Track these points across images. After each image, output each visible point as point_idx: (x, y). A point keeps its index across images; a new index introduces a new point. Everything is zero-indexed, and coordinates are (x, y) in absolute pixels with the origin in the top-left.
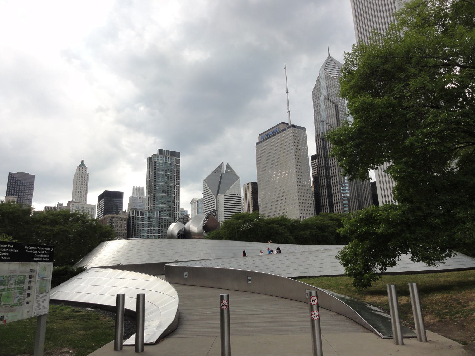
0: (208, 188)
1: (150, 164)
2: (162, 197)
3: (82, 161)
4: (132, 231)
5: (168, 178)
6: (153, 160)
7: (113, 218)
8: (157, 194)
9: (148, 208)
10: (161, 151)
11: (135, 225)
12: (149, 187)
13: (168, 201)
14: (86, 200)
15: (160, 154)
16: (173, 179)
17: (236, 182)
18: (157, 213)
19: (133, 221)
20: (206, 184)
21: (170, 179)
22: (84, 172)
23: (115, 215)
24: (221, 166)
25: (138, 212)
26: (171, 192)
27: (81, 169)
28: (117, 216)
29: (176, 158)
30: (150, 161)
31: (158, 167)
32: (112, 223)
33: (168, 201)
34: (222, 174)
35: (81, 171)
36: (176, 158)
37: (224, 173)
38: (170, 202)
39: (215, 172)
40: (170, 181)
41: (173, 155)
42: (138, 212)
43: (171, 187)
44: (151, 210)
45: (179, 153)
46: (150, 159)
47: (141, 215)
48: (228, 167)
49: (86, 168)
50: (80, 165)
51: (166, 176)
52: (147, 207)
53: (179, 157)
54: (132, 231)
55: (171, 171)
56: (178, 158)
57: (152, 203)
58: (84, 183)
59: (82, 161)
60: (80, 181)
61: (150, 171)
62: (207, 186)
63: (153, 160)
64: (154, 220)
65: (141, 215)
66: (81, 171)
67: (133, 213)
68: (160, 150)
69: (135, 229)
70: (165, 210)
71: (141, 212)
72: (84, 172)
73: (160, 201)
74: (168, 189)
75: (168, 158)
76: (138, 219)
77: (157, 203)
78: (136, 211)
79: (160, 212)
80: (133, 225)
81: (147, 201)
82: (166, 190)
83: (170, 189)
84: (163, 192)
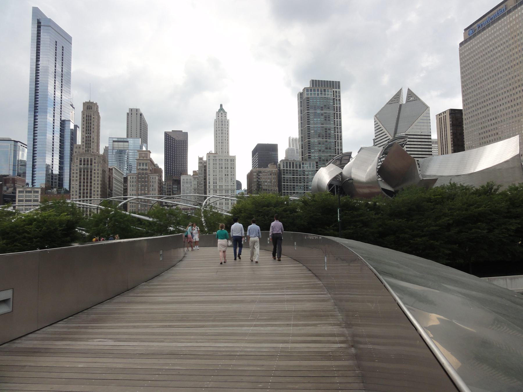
0: (381, 126)
1: (301, 102)
2: (319, 144)
3: (221, 106)
4: (284, 187)
5: (325, 117)
6: (305, 96)
7: (260, 172)
8: (312, 140)
9: (302, 158)
10: (314, 83)
11: (287, 180)
12: (302, 132)
13: (326, 148)
14: (228, 152)
15: (313, 85)
16: (332, 118)
17: (424, 114)
18: (313, 164)
19: (284, 175)
20: (378, 121)
21: (327, 119)
22: (223, 118)
23: (262, 169)
24: (398, 96)
25: (290, 163)
26: (329, 137)
27: (220, 115)
28: (265, 169)
29: (335, 90)
30: (301, 98)
31: (311, 104)
32: (259, 179)
33: (326, 148)
34: (401, 105)
35: (220, 118)
36: (335, 90)
37: (404, 102)
38: (330, 149)
39: (391, 102)
40: (328, 122)
41: (330, 86)
42: (290, 163)
43: (329, 129)
44: (306, 160)
45: (339, 82)
46: (301, 95)
47: (293, 168)
48: (410, 94)
49: (225, 113)
50: (220, 110)
51: (322, 115)
52: (301, 157)
53: (339, 88)
54: (284, 187)
55: (329, 108)
56: (337, 90)
57: (307, 151)
58: (224, 132)
59: (221, 106)
60: (220, 129)
61: (301, 111)
62: (379, 123)
63: (305, 96)
64: (310, 173)
65: (293, 168)
66: (220, 118)
67: (284, 166)
68: (313, 81)
69: (287, 185)
70: (323, 160)
71: (293, 163)
72: (223, 118)
73: (316, 148)
74: (326, 132)
75: (325, 90)
76: (290, 173)
77: (313, 151)
78: (287, 163)
79: (317, 163)
80: (284, 180)
81: (301, 150)
82: (324, 134)
83: (328, 131)
84: (319, 136)
